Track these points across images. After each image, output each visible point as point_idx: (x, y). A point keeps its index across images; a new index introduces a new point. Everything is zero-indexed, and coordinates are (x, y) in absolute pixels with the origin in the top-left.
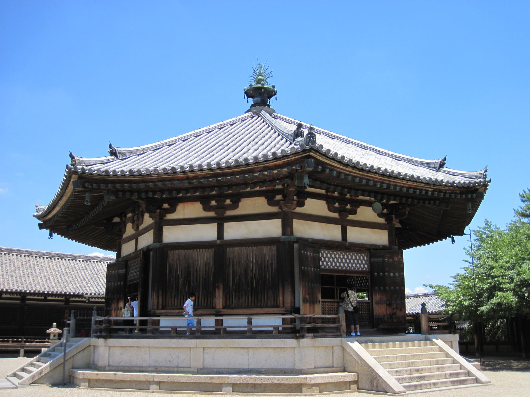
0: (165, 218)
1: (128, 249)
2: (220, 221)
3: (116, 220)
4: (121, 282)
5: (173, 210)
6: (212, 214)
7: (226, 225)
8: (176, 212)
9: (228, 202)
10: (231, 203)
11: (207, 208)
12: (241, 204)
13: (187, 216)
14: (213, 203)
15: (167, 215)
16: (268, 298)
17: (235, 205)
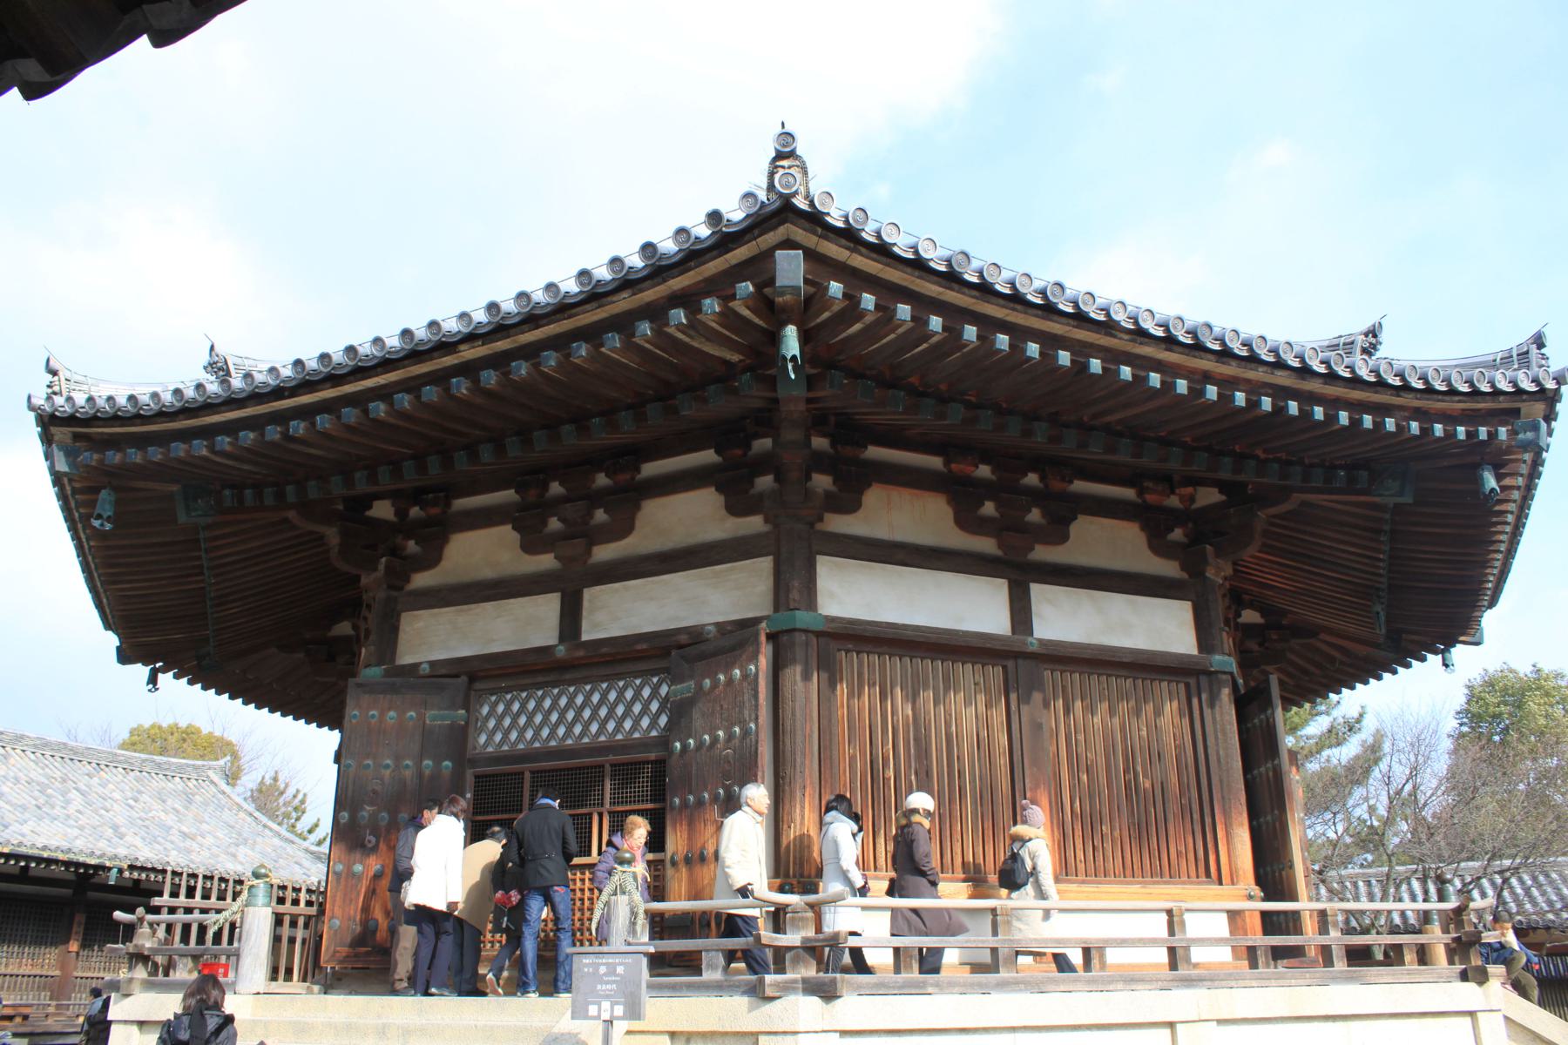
0: (819, 526)
1: (433, 637)
2: (1021, 576)
3: (383, 510)
4: (438, 762)
5: (847, 501)
6: (986, 545)
7: (1036, 589)
8: (860, 514)
9: (1035, 515)
10: (1043, 521)
11: (966, 520)
12: (1074, 528)
13: (899, 536)
14: (989, 508)
15: (828, 516)
16: (1178, 854)
17: (1057, 531)
